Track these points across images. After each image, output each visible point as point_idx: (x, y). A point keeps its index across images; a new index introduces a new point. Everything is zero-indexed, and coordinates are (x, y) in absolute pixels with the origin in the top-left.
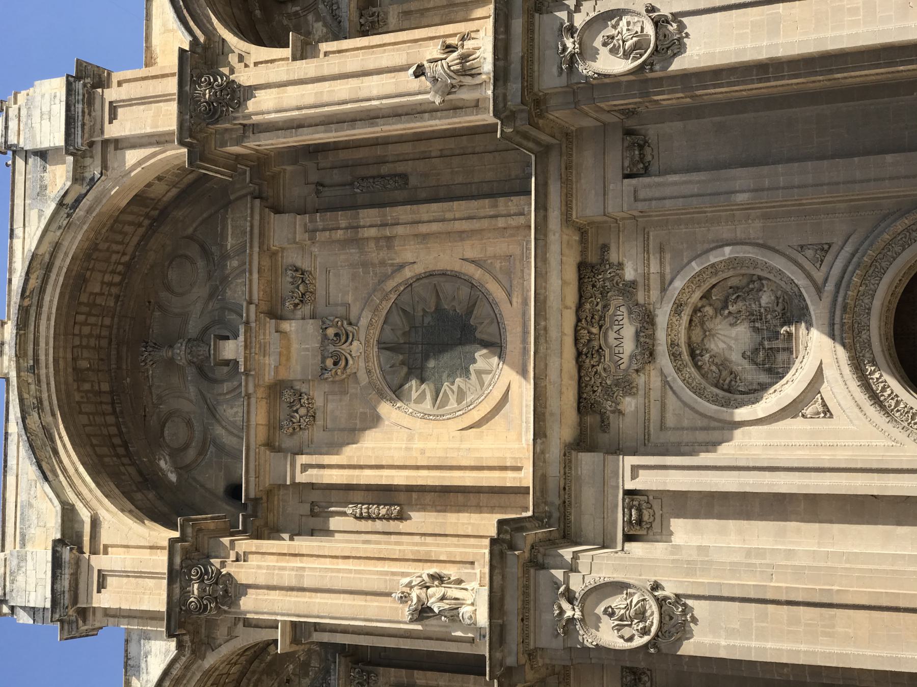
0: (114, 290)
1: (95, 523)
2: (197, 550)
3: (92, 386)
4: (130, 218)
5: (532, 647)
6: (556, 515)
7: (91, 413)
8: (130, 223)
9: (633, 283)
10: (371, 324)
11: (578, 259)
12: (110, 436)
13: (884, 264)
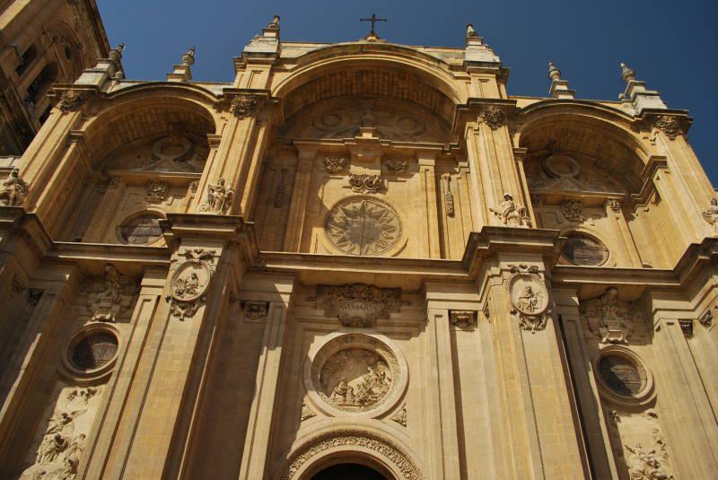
0: (400, 95)
1: (286, 71)
2: (266, 105)
4: (434, 98)
5: (183, 239)
6: (260, 265)
8: (431, 100)
9: (388, 318)
10: (378, 199)
11: (404, 288)
12: (330, 91)
13: (391, 457)
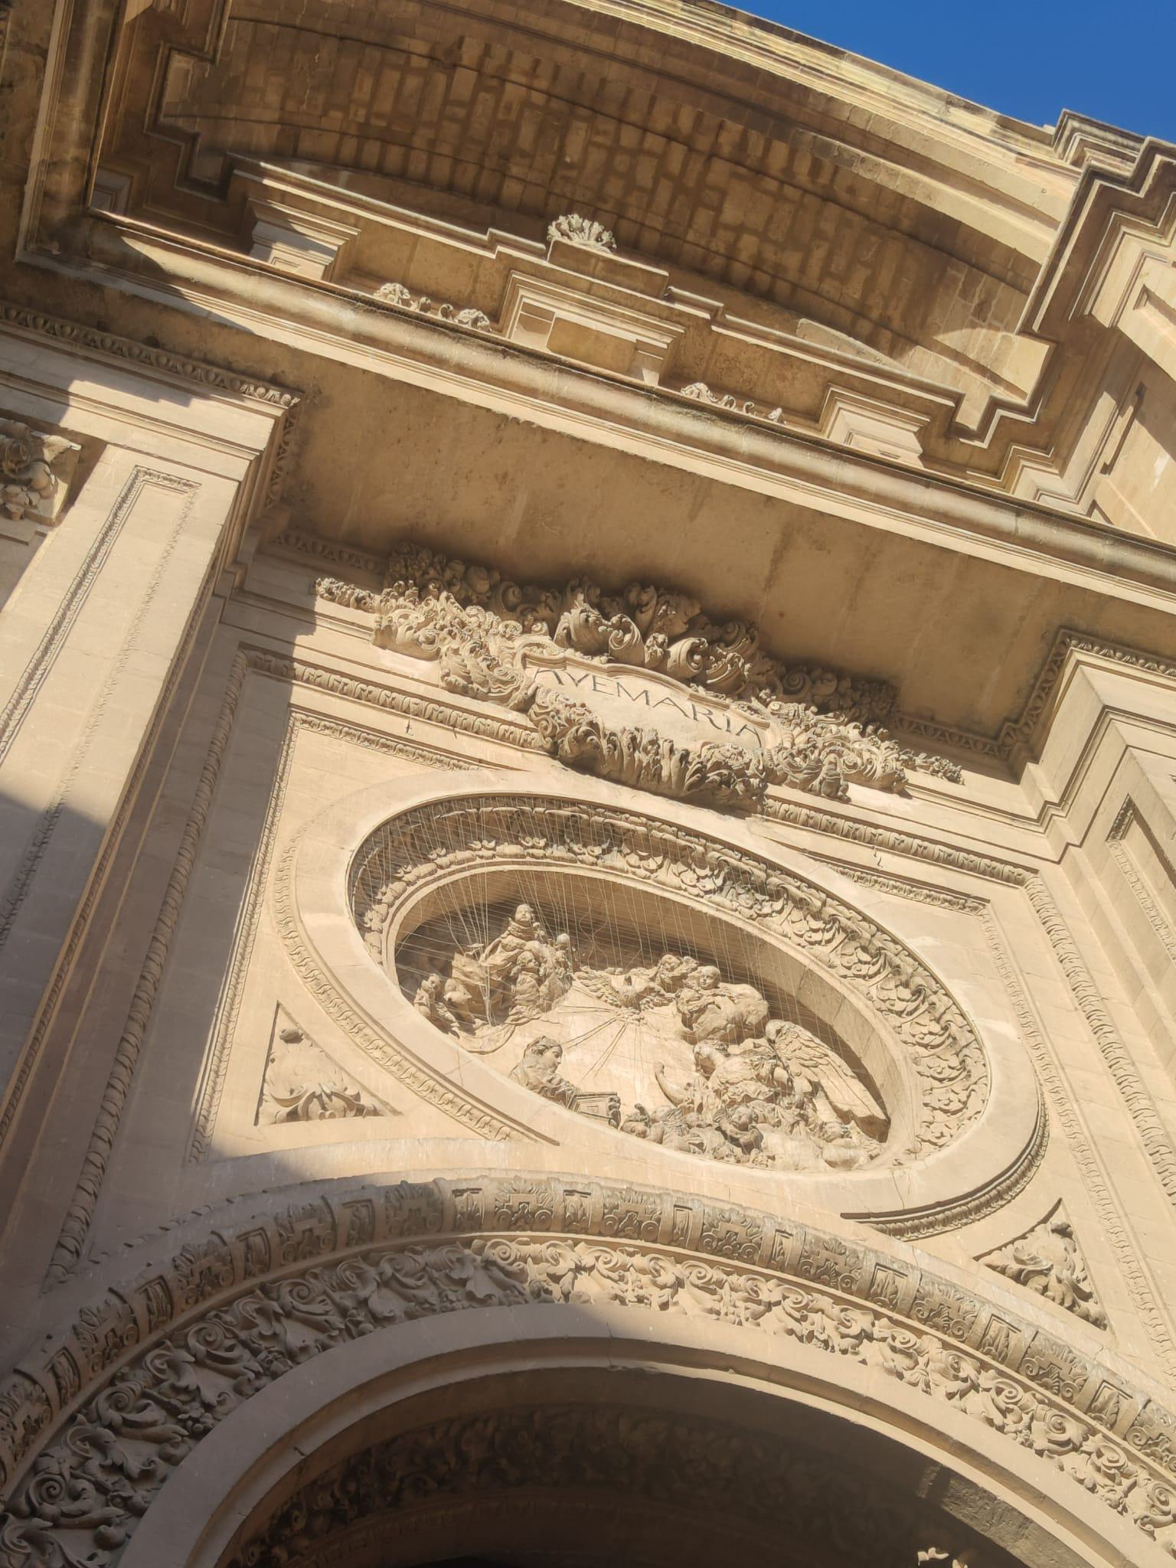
3: (523, 154)
4: (885, 278)
7: (469, 116)
9: (835, 791)
